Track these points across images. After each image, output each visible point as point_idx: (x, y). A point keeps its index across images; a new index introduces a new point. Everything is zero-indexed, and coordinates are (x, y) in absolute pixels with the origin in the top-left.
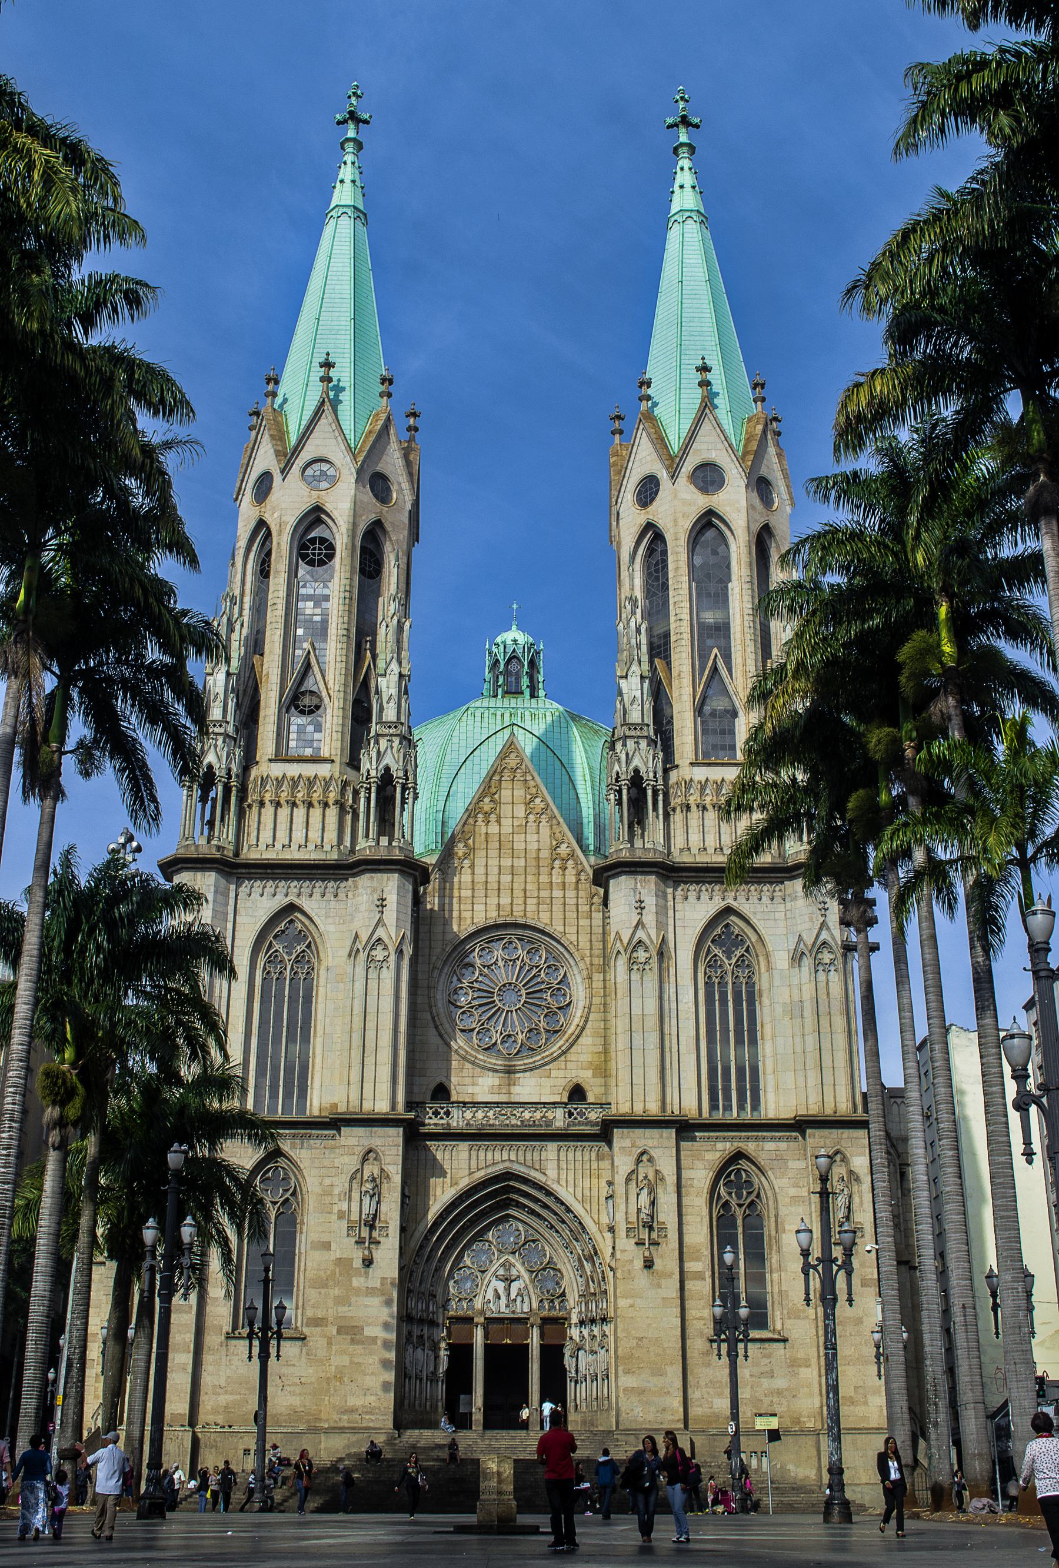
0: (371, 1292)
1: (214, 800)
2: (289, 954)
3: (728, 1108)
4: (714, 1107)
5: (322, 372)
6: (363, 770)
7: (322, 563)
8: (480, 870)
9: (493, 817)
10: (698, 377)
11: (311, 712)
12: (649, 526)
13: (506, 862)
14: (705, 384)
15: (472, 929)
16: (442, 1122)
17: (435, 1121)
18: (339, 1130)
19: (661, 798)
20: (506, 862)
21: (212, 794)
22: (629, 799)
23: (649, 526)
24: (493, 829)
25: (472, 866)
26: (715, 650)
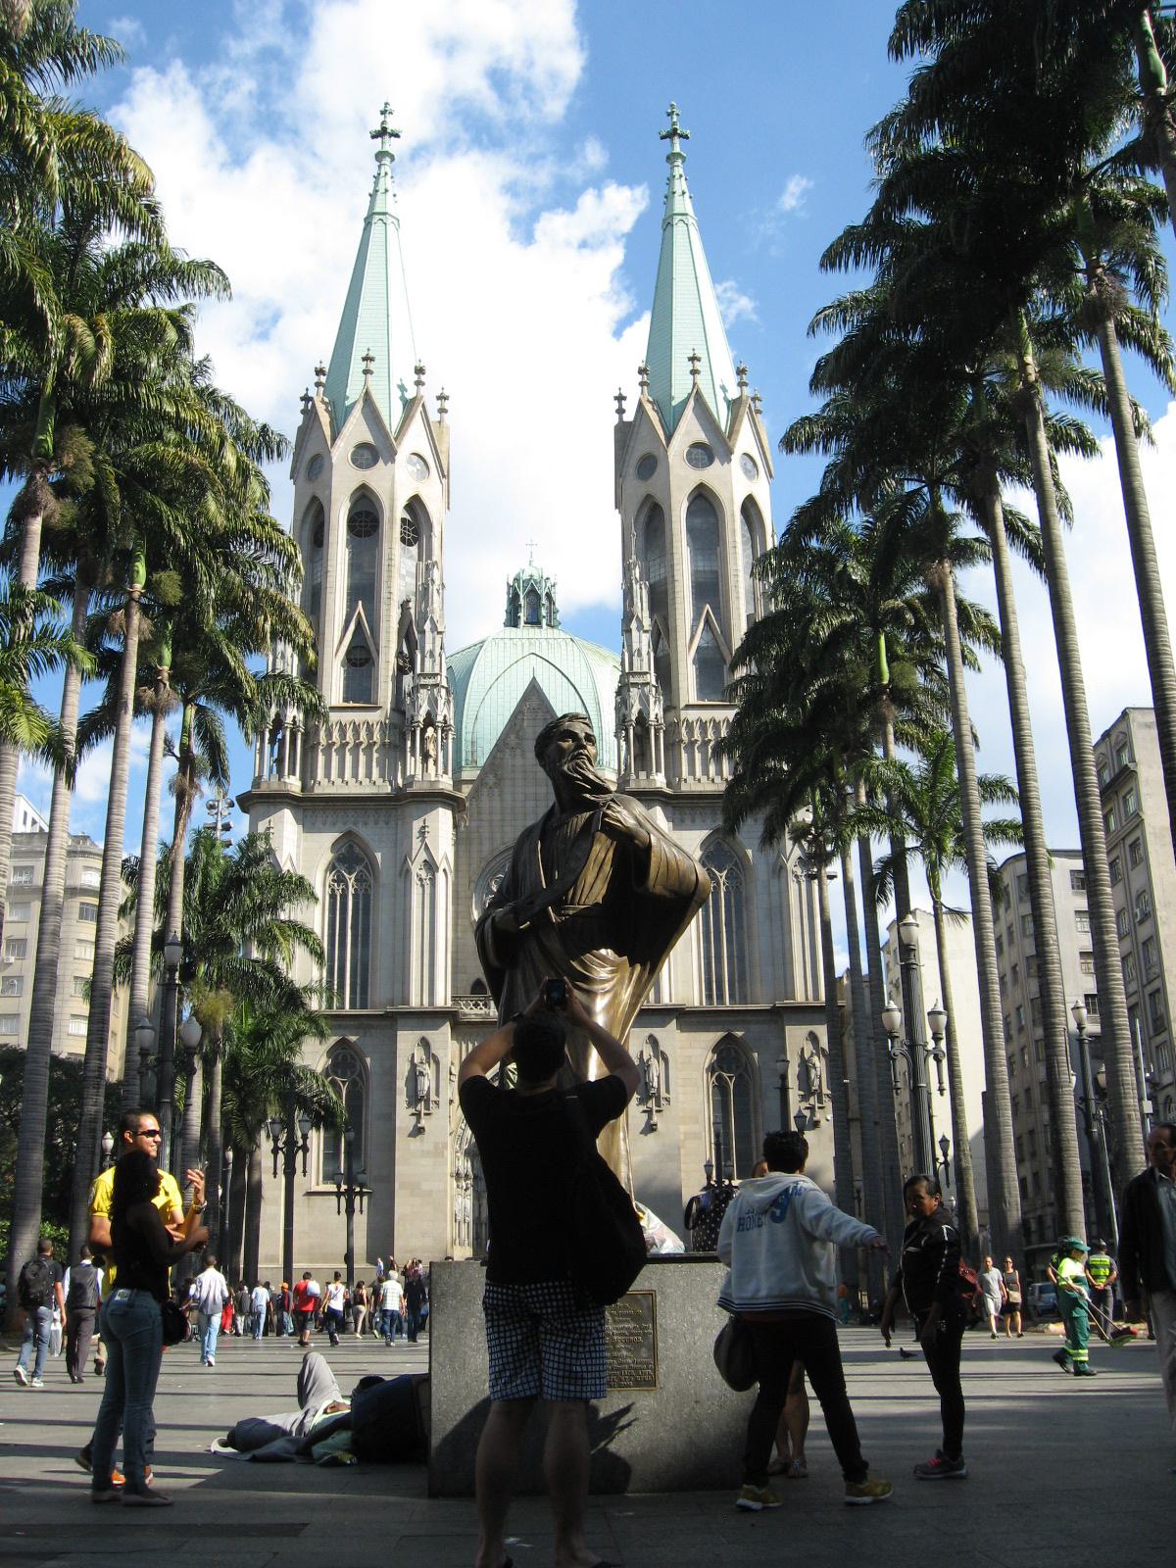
0: (425, 1154)
1: (282, 742)
2: (350, 873)
3: (721, 997)
4: (709, 997)
5: (363, 365)
6: (408, 715)
7: (368, 534)
8: (508, 797)
9: (518, 751)
10: (689, 366)
11: (361, 665)
12: (648, 497)
13: (531, 790)
14: (694, 372)
15: (502, 848)
16: (482, 1012)
17: (476, 1011)
18: (396, 1021)
19: (662, 735)
20: (531, 790)
21: (280, 736)
22: (635, 734)
23: (648, 497)
24: (519, 761)
25: (501, 794)
26: (708, 606)
